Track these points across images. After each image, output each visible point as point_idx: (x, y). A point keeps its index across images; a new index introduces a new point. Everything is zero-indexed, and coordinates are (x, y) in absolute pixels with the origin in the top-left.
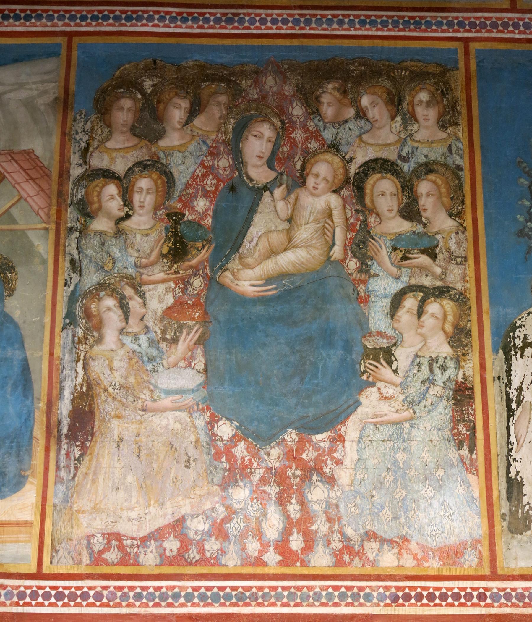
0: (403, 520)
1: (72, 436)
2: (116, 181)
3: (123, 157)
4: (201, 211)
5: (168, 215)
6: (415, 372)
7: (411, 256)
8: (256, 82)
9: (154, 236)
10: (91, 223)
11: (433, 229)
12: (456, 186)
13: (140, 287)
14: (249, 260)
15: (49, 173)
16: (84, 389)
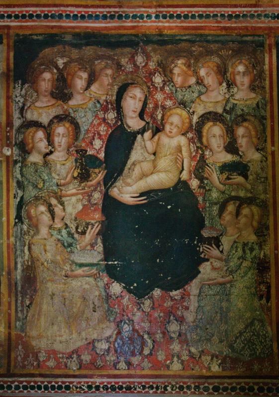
2: (42, 129)
3: (46, 112)
4: (98, 149)
5: (77, 151)
6: (234, 252)
7: (232, 177)
10: (28, 157)
13: (61, 199)
16: (30, 263)
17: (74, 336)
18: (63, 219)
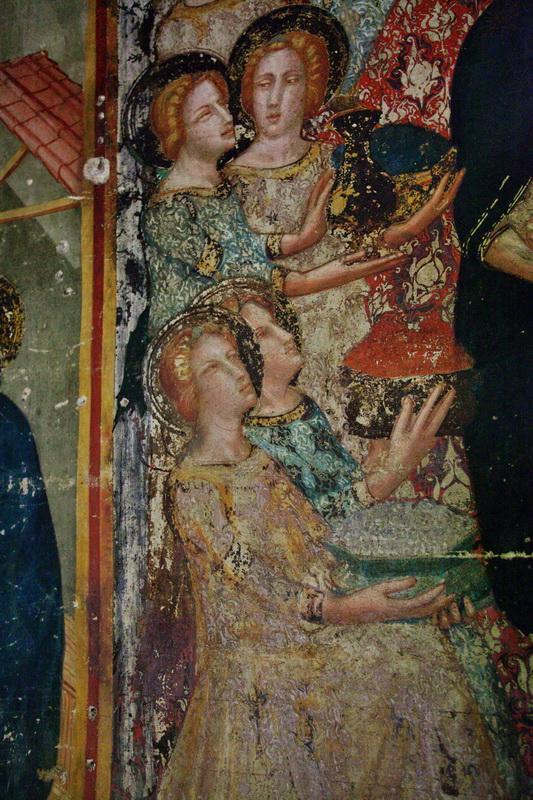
4: (421, 96)
5: (340, 123)
9: (308, 175)
10: (166, 176)
13: (284, 303)
15: (74, 89)
16: (169, 563)
18: (293, 382)
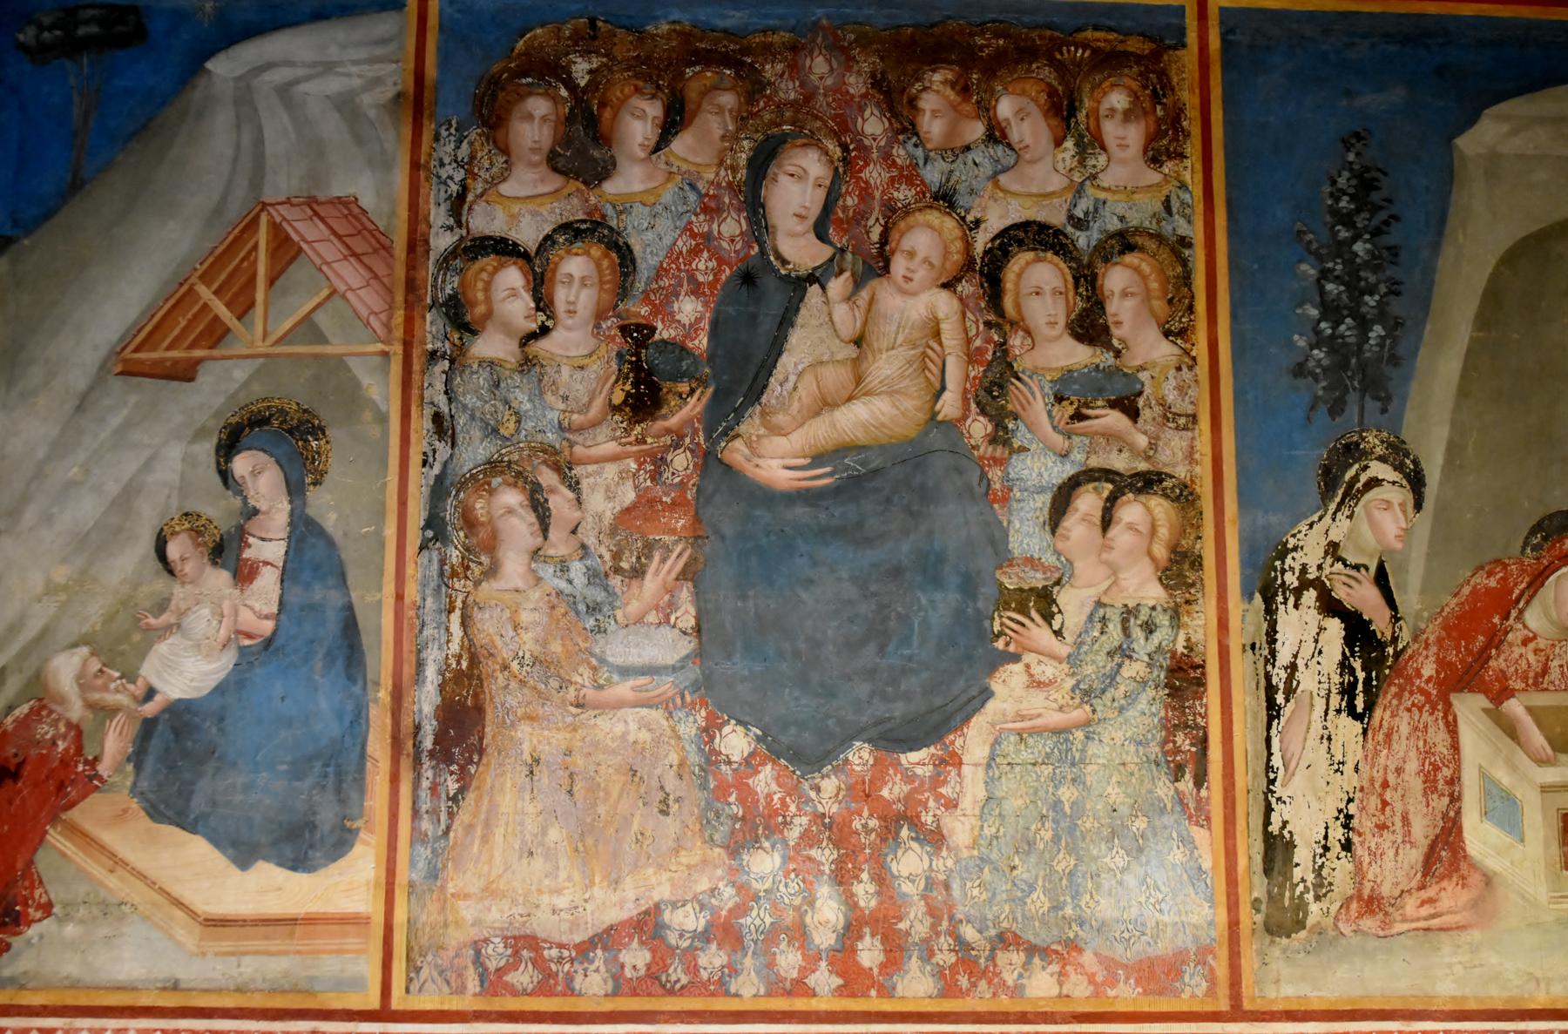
0: (1069, 911)
1: (443, 753)
2: (520, 262)
3: (534, 214)
4: (687, 322)
5: (625, 330)
6: (1096, 634)
8: (794, 69)
9: (595, 368)
11: (1132, 360)
12: (1177, 277)
13: (570, 469)
14: (780, 419)
15: (388, 243)
16: (464, 665)
17: (598, 892)
18: (574, 532)
